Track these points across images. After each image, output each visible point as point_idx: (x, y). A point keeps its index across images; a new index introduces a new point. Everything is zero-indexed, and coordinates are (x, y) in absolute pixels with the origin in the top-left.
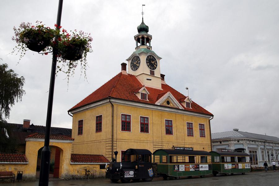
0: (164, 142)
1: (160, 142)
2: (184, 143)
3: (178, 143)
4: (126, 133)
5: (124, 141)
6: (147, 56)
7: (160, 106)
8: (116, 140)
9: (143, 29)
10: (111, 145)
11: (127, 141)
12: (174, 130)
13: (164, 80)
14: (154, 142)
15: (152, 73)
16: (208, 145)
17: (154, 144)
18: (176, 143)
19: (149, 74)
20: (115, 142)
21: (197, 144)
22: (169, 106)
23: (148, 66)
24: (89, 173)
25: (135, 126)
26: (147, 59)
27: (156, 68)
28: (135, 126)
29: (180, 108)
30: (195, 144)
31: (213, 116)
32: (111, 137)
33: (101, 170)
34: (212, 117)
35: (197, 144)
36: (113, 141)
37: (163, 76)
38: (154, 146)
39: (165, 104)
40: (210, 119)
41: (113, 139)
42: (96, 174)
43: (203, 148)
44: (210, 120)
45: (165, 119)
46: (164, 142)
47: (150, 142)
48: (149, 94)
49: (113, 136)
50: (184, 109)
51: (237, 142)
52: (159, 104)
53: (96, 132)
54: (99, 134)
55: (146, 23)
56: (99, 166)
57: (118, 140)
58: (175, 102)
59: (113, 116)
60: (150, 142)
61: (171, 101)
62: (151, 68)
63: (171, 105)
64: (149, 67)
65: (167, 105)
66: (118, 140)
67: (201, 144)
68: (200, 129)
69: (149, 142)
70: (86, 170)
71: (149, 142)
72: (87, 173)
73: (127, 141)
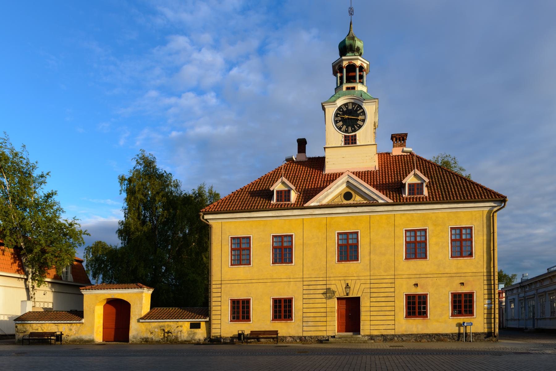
0: (332, 279)
1: (321, 279)
2: (393, 277)
4: (241, 270)
5: (236, 282)
11: (243, 282)
12: (363, 250)
17: (305, 283)
21: (440, 275)
22: (351, 202)
24: (170, 334)
25: (261, 252)
28: (261, 252)
29: (380, 201)
30: (429, 276)
33: (192, 330)
35: (440, 275)
38: (305, 287)
42: (181, 336)
50: (390, 201)
65: (346, 202)
67: (453, 275)
68: (452, 240)
70: (164, 330)
71: (292, 280)
72: (166, 335)
73: (243, 282)
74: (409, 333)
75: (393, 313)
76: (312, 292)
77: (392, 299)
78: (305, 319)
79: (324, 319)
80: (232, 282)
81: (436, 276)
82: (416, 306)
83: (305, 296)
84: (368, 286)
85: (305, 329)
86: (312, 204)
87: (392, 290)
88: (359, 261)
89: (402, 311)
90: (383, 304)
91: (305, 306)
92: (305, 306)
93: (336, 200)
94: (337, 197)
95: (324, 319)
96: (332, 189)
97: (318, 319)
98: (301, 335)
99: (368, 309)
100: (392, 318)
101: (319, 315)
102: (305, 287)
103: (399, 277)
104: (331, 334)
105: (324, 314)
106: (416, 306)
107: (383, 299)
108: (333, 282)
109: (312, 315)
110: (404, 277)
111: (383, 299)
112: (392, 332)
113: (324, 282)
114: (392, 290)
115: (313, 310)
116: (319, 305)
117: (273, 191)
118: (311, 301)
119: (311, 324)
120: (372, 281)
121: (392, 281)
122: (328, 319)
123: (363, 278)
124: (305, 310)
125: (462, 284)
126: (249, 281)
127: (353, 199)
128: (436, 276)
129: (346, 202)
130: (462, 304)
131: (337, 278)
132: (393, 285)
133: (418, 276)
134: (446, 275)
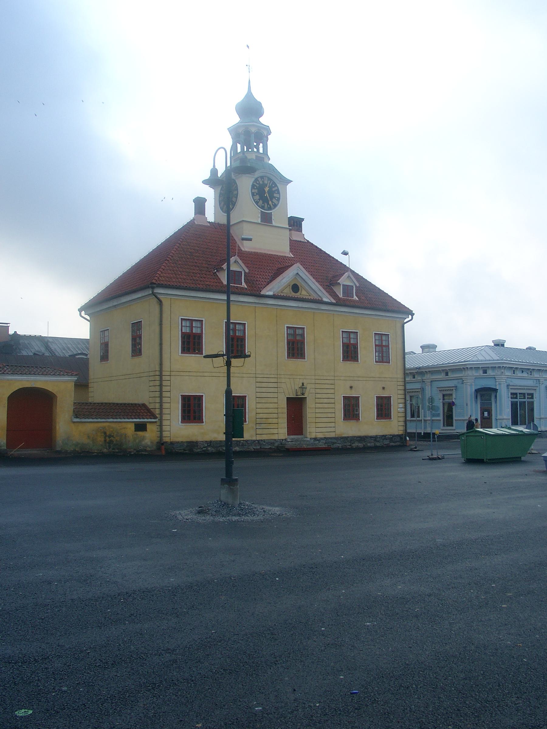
0: (282, 376)
1: (273, 376)
2: (333, 378)
3: (317, 377)
5: (187, 374)
6: (253, 179)
8: (168, 373)
9: (250, 109)
10: (158, 383)
11: (195, 374)
12: (308, 349)
13: (301, 231)
14: (257, 376)
15: (266, 219)
16: (395, 380)
18: (313, 377)
19: (259, 221)
20: (168, 378)
22: (297, 295)
23: (257, 203)
24: (112, 438)
26: (253, 187)
27: (275, 206)
29: (325, 300)
30: (360, 379)
31: (412, 315)
32: (158, 368)
34: (410, 316)
36: (161, 376)
37: (296, 224)
38: (258, 385)
39: (288, 292)
40: (405, 321)
41: (161, 371)
44: (405, 325)
45: (286, 326)
46: (282, 376)
47: (248, 375)
48: (247, 271)
49: (161, 364)
50: (334, 301)
51: (481, 372)
52: (271, 293)
53: (132, 356)
54: (137, 360)
55: (258, 96)
56: (132, 427)
57: (173, 373)
58: (313, 286)
59: (161, 324)
60: (248, 375)
61: (303, 284)
62: (263, 207)
63: (303, 293)
64: (259, 204)
65: (293, 294)
66: (173, 373)
69: (245, 375)
70: (105, 433)
71: (245, 375)
72: (108, 439)
73: (195, 374)
75: (333, 415)
77: (332, 401)
78: (259, 421)
79: (275, 421)
80: (182, 374)
82: (351, 409)
83: (259, 395)
85: (259, 431)
86: (267, 294)
87: (332, 391)
89: (340, 413)
92: (259, 406)
93: (285, 291)
97: (270, 421)
98: (254, 438)
102: (258, 385)
105: (275, 416)
106: (351, 409)
107: (326, 401)
108: (283, 380)
110: (342, 378)
112: (332, 435)
113: (275, 380)
114: (332, 391)
118: (263, 400)
120: (317, 381)
121: (332, 382)
124: (259, 411)
125: (384, 388)
126: (201, 374)
128: (364, 379)
130: (383, 409)
131: (286, 376)
132: (332, 387)
133: (352, 378)
134: (372, 379)
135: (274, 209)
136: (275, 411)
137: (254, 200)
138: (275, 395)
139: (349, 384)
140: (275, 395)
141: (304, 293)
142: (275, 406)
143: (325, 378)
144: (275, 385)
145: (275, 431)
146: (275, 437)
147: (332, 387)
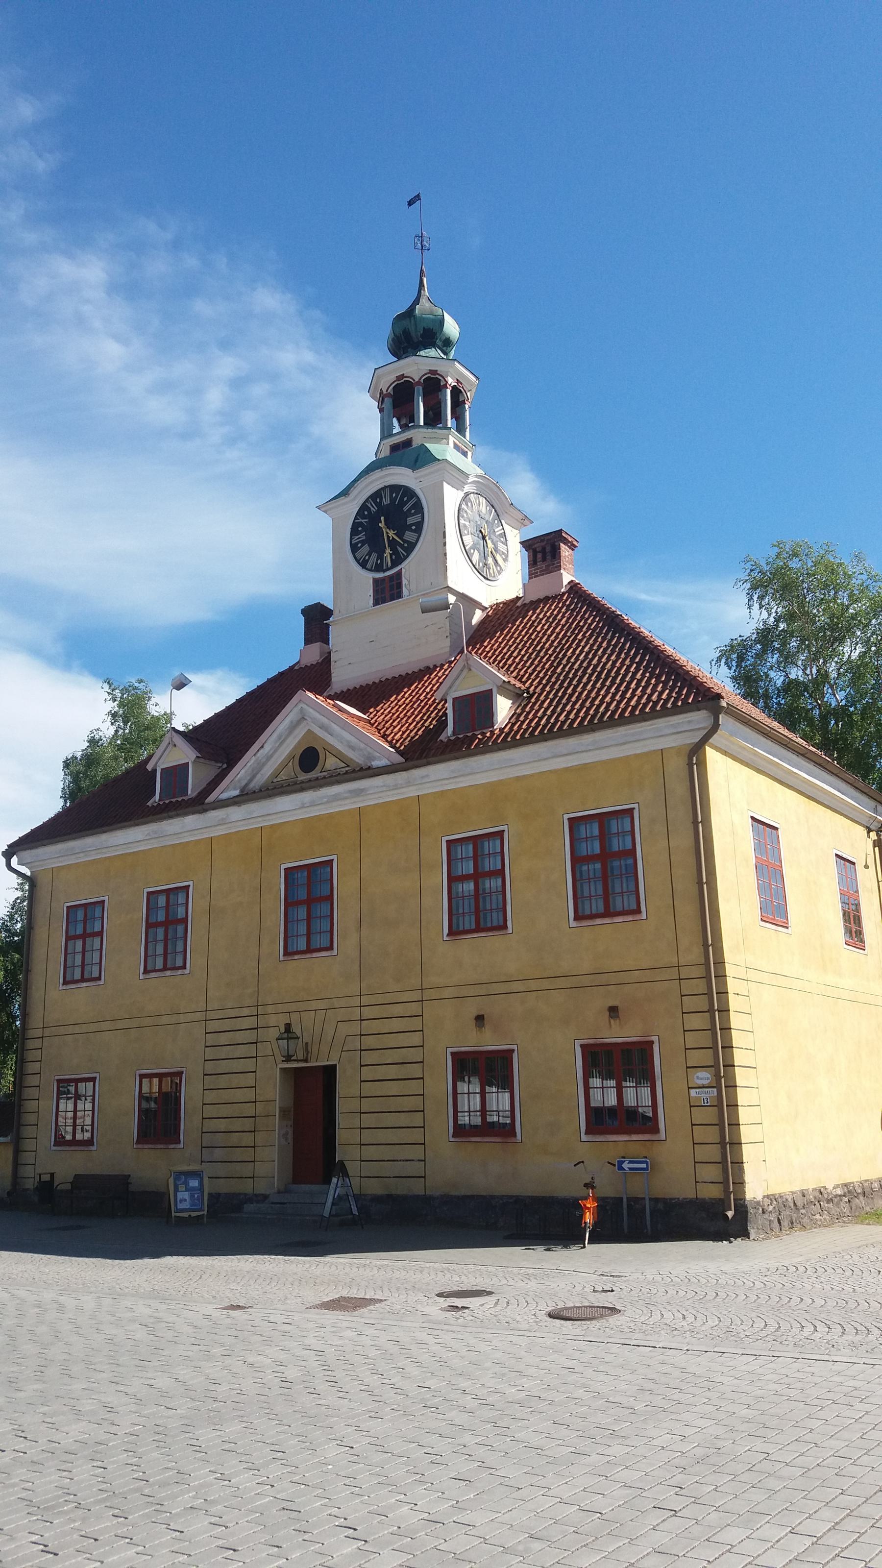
0: (270, 1009)
1: (246, 1012)
2: (416, 996)
3: (365, 1000)
5: (71, 1029)
7: (247, 796)
8: (38, 1033)
15: (388, 591)
17: (213, 1026)
21: (546, 984)
30: (516, 987)
35: (546, 984)
43: (613, 1011)
45: (283, 867)
46: (270, 1009)
47: (191, 1017)
60: (191, 1017)
62: (378, 568)
67: (586, 981)
74: (463, 1192)
75: (417, 1119)
76: (223, 1052)
77: (415, 1071)
79: (247, 1139)
81: (533, 985)
83: (210, 1067)
84: (355, 1028)
86: (224, 796)
87: (416, 1039)
88: (335, 952)
90: (393, 1088)
91: (210, 1097)
92: (210, 1097)
93: (283, 776)
94: (284, 766)
95: (247, 1139)
96: (267, 747)
97: (234, 1139)
99: (354, 1105)
100: (416, 1136)
101: (237, 1125)
103: (433, 994)
104: (261, 1188)
105: (248, 1124)
107: (393, 1072)
109: (222, 1125)
110: (447, 993)
111: (393, 1072)
112: (417, 1188)
114: (416, 1039)
115: (225, 1111)
116: (239, 1095)
117: (154, 771)
119: (218, 1154)
120: (367, 1012)
121: (414, 1009)
122: (260, 1138)
123: (343, 1003)
124: (210, 1111)
125: (613, 1011)
126: (93, 1027)
127: (319, 768)
128: (533, 985)
129: (303, 777)
132: (416, 1023)
134: (562, 983)
135: (406, 558)
136: (249, 1110)
137: (357, 561)
138: (250, 1065)
139: (471, 1010)
140: (250, 1065)
141: (331, 763)
142: (250, 1095)
143: (389, 998)
144: (250, 1036)
145: (247, 1170)
146: (247, 1187)
147: (416, 1023)
